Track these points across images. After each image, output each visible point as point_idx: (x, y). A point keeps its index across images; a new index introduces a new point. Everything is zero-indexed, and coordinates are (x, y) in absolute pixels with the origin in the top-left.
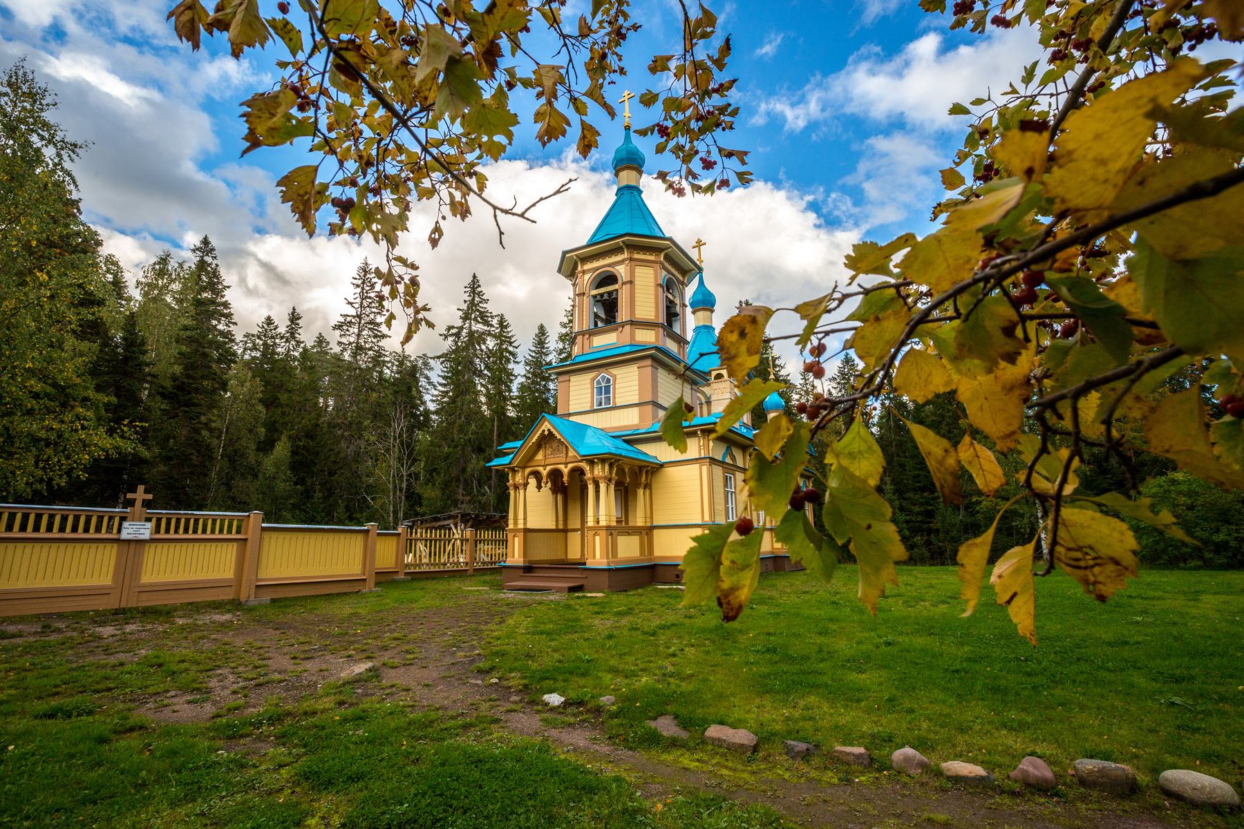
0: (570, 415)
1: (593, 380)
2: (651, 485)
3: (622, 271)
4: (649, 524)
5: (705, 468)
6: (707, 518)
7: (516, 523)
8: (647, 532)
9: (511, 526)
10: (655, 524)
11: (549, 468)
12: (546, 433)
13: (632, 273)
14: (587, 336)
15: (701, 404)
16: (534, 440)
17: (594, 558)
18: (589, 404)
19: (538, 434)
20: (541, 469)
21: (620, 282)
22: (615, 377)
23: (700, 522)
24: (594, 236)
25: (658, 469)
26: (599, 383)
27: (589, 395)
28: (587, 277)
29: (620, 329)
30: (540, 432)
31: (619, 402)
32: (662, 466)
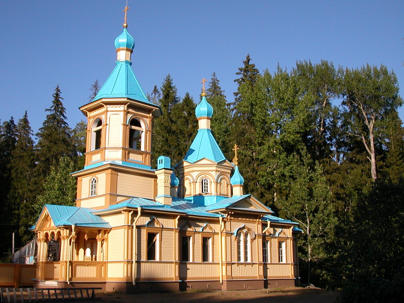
0: (81, 200)
2: (107, 239)
3: (103, 117)
5: (126, 231)
6: (126, 258)
10: (109, 261)
11: (51, 231)
12: (47, 214)
14: (89, 155)
15: (190, 183)
16: (43, 218)
18: (88, 194)
19: (44, 215)
21: (102, 124)
22: (98, 178)
23: (123, 260)
25: (110, 231)
27: (88, 189)
28: (91, 120)
29: (101, 152)
30: (45, 213)
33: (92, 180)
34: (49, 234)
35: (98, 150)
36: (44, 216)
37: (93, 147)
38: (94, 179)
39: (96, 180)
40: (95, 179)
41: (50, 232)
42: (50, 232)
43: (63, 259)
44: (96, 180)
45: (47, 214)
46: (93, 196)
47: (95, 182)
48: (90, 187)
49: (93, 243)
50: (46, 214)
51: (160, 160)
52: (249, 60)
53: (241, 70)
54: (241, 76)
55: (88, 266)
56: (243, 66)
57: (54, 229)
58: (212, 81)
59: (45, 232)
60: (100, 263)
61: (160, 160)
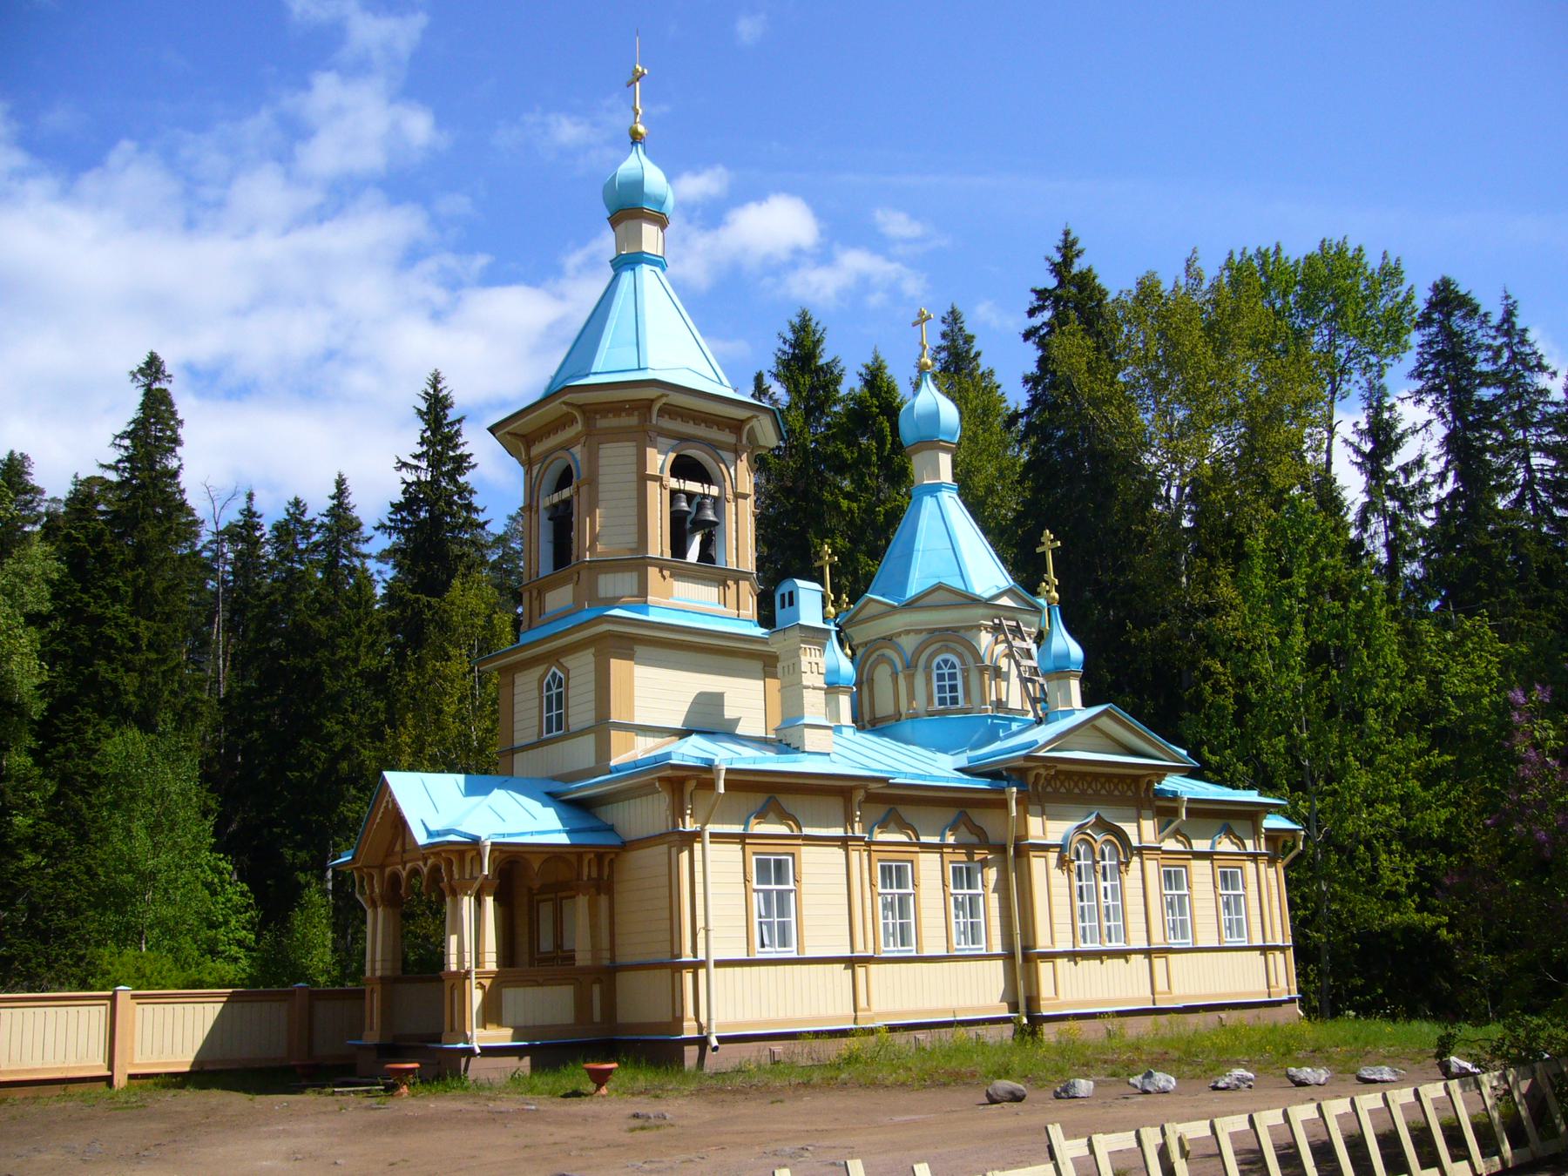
1: (541, 680)
4: (606, 962)
7: (373, 970)
8: (608, 974)
9: (368, 974)
11: (409, 866)
13: (593, 458)
17: (371, 1029)
20: (400, 867)
22: (567, 672)
24: (554, 379)
25: (617, 854)
26: (549, 688)
27: (536, 712)
30: (384, 805)
31: (573, 728)
32: (626, 846)
33: (549, 676)
34: (404, 874)
35: (563, 572)
36: (380, 816)
37: (546, 565)
38: (555, 674)
39: (562, 676)
40: (559, 674)
41: (404, 869)
42: (404, 869)
43: (373, 970)
44: (560, 678)
45: (390, 806)
46: (555, 733)
47: (560, 686)
48: (541, 702)
49: (561, 903)
50: (386, 807)
51: (783, 595)
52: (1067, 261)
53: (1041, 294)
54: (1047, 315)
55: (539, 985)
56: (1051, 282)
57: (419, 860)
58: (944, 343)
59: (388, 870)
60: (584, 970)
61: (783, 595)
